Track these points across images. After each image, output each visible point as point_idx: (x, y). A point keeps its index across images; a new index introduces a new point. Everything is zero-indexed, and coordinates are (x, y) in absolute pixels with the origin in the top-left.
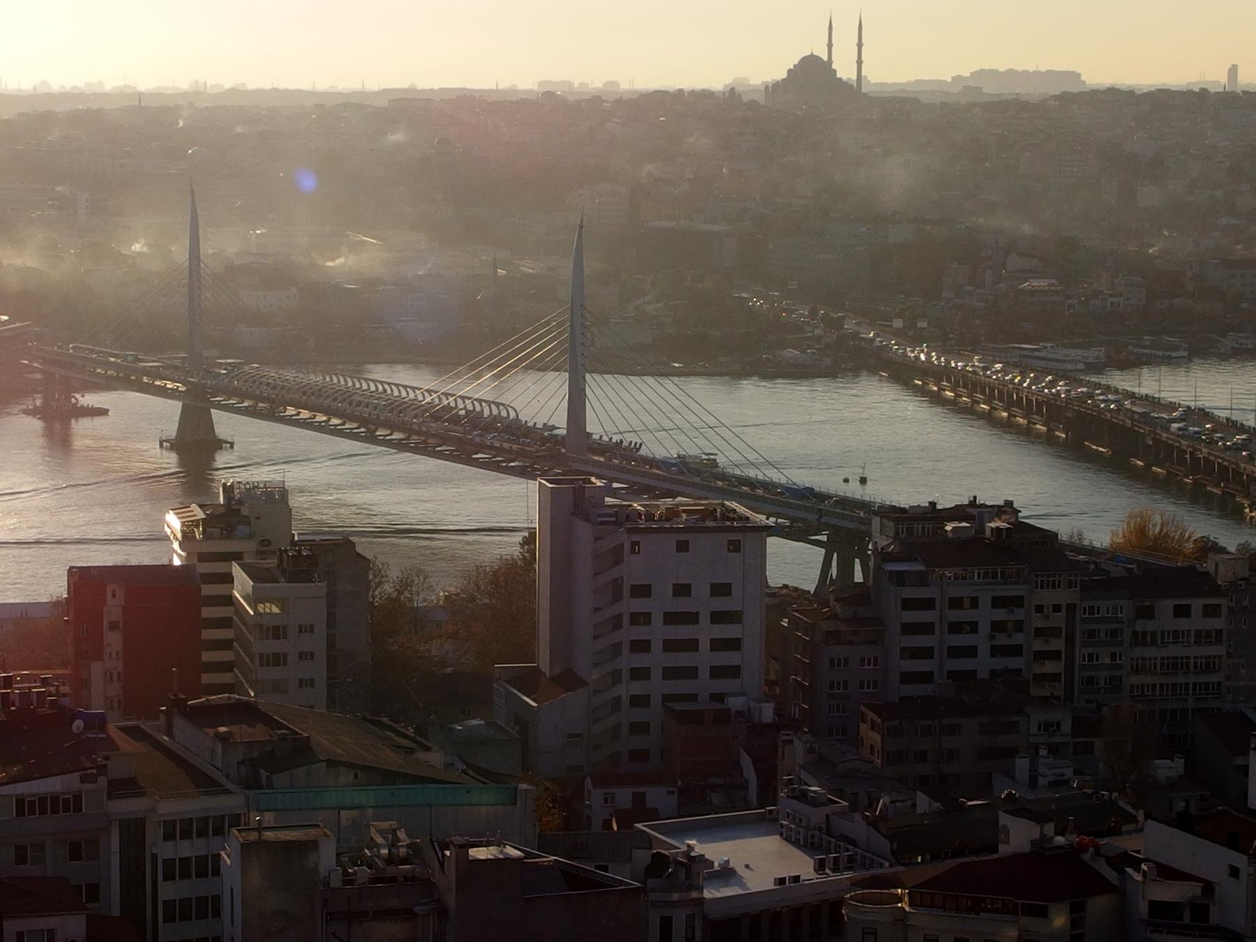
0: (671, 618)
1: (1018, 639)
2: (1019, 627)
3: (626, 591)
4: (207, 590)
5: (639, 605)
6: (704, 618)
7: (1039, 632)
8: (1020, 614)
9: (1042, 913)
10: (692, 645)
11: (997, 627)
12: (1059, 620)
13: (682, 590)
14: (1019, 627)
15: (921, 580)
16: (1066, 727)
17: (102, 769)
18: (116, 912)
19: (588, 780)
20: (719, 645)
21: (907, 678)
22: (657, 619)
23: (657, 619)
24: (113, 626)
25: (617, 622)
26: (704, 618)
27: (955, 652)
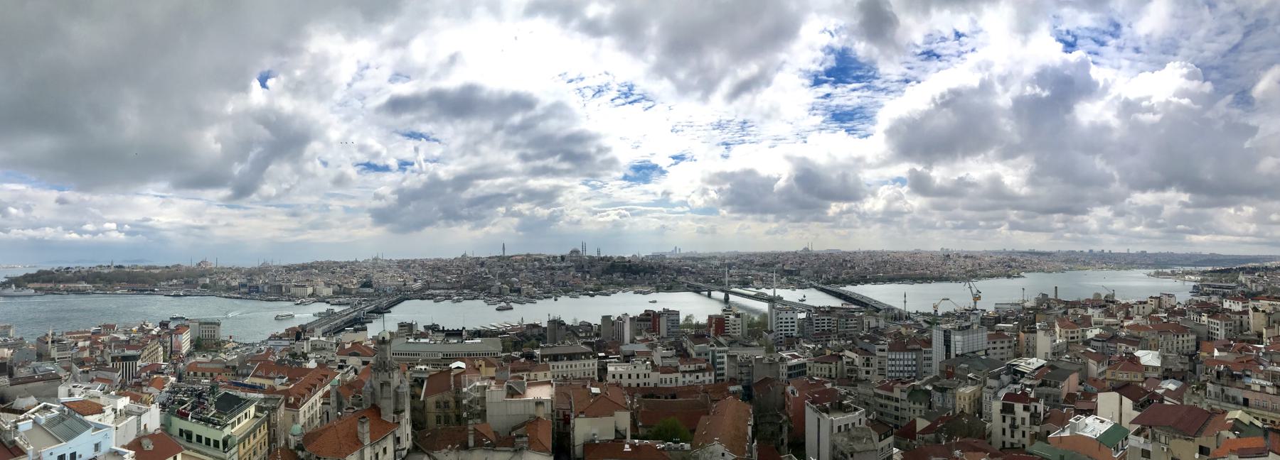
0: (785, 323)
13: (787, 319)
20: (791, 326)
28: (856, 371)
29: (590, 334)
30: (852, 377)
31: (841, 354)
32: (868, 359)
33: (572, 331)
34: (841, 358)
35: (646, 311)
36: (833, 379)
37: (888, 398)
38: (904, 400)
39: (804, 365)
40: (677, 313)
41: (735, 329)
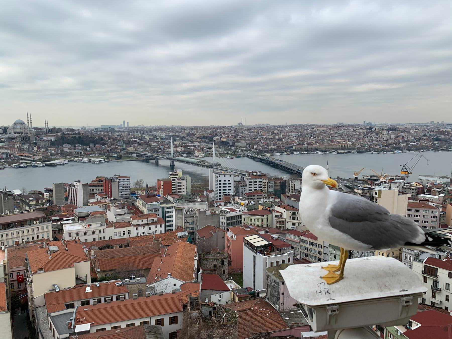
0: (223, 184)
1: (262, 186)
2: (261, 184)
3: (219, 181)
4: (173, 181)
5: (220, 182)
6: (227, 184)
7: (264, 185)
8: (262, 183)
9: (264, 216)
10: (226, 187)
11: (259, 184)
12: (266, 184)
13: (225, 181)
14: (261, 184)
15: (251, 179)
16: (267, 195)
17: (160, 201)
18: (161, 217)
19: (215, 202)
20: (229, 187)
21: (249, 190)
22: (222, 184)
23: (222, 184)
24: (162, 185)
25: (218, 184)
26: (227, 184)
27: (255, 187)
28: (283, 222)
29: (42, 201)
30: (280, 227)
31: (271, 209)
32: (294, 214)
33: (21, 200)
34: (271, 212)
35: (98, 177)
36: (265, 228)
37: (313, 244)
38: (327, 247)
39: (240, 216)
40: (128, 179)
41: (180, 189)
